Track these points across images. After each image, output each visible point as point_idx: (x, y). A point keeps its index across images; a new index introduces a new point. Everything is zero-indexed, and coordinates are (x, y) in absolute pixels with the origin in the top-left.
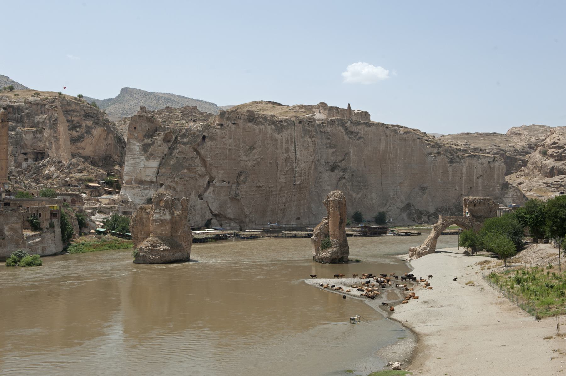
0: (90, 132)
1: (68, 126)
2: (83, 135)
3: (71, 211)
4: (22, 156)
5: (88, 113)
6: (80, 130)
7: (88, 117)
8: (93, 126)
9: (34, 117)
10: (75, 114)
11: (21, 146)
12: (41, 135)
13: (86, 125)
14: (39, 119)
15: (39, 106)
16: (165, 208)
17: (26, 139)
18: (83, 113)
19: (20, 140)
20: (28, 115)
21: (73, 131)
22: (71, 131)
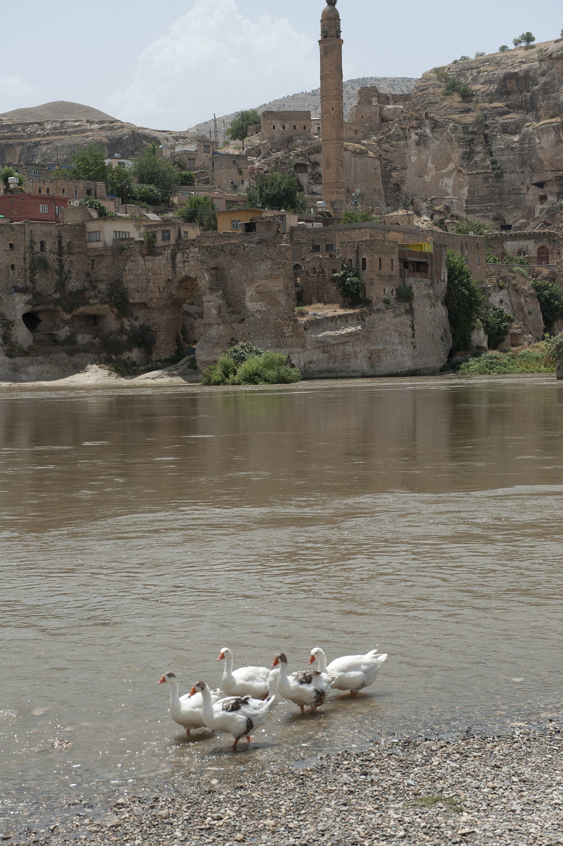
3: (522, 275)
11: (531, 166)
19: (529, 153)
20: (547, 89)
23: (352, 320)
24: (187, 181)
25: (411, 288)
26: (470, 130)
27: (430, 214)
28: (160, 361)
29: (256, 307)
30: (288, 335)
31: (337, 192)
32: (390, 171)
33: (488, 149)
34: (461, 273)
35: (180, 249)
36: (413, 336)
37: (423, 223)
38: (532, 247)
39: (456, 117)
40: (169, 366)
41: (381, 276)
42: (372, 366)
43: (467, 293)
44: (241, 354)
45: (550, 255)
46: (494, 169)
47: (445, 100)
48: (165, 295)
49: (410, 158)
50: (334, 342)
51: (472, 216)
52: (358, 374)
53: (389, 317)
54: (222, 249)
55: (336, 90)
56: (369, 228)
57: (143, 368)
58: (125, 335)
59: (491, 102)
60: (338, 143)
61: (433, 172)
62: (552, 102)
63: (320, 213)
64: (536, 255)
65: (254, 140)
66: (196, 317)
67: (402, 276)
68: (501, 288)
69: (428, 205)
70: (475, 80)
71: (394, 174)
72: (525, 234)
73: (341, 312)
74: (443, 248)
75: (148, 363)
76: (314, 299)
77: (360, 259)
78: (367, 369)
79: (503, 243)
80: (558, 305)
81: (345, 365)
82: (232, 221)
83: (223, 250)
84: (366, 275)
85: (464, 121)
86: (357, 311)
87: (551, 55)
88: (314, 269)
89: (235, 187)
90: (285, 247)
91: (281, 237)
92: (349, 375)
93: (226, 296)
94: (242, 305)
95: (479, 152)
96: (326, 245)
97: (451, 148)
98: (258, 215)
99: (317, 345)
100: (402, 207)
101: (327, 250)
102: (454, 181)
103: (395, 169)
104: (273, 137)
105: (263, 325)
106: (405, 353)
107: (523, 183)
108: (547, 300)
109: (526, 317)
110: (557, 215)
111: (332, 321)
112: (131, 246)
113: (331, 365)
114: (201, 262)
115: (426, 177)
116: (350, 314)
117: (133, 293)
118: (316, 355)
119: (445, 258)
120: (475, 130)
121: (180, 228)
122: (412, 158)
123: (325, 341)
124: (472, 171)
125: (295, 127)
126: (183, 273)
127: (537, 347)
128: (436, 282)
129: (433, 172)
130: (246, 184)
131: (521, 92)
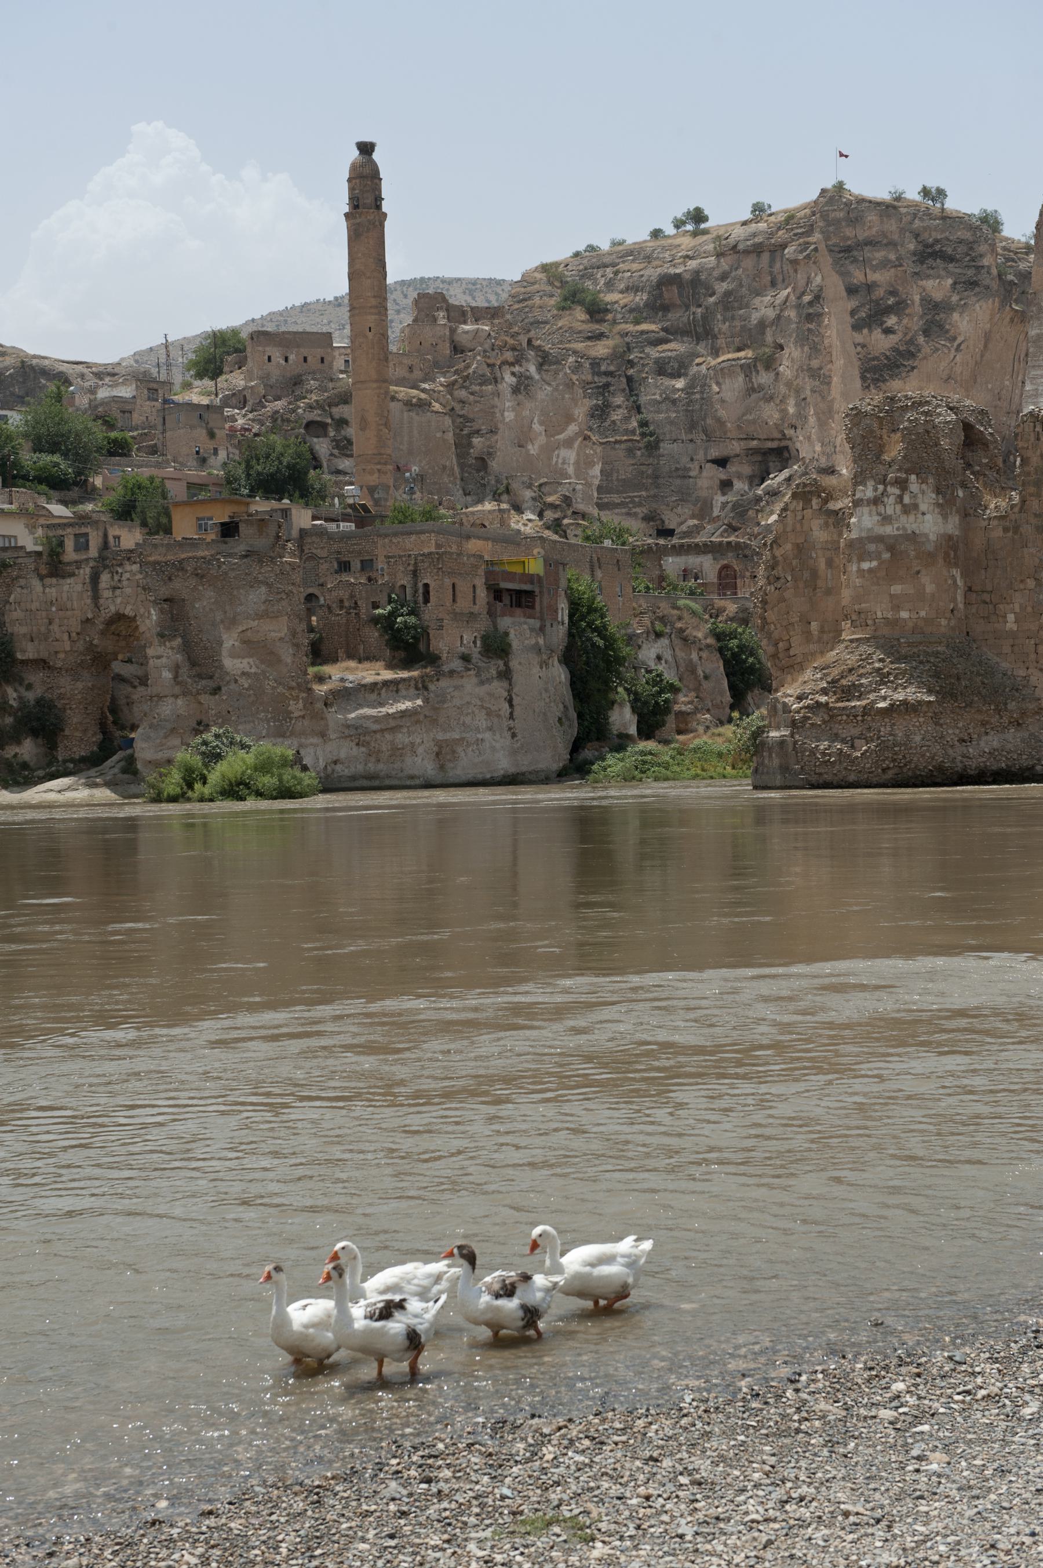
0: (941, 327)
1: (853, 313)
2: (911, 342)
3: (694, 613)
4: (711, 470)
5: (932, 246)
6: (898, 323)
7: (930, 261)
8: (955, 298)
9: (747, 306)
10: (880, 255)
11: (705, 431)
12: (772, 375)
13: (922, 300)
14: (763, 311)
15: (766, 257)
16: (908, 472)
17: (723, 401)
18: (912, 247)
19: (701, 409)
20: (730, 303)
21: (870, 331)
22: (865, 331)
23: (407, 689)
24: (118, 449)
25: (507, 634)
26: (603, 368)
27: (538, 509)
28: (72, 760)
29: (242, 666)
30: (296, 714)
31: (379, 470)
32: (470, 436)
33: (634, 402)
34: (591, 610)
35: (105, 567)
36: (511, 716)
37: (525, 525)
38: (709, 566)
39: (579, 346)
40: (89, 769)
41: (455, 614)
42: (442, 767)
43: (601, 643)
44: (214, 748)
45: (738, 581)
46: (643, 435)
47: (560, 317)
48: (80, 646)
49: (502, 415)
50: (376, 727)
51: (608, 512)
52: (417, 782)
53: (470, 683)
54: (180, 566)
55: (375, 297)
56: (434, 532)
57: (40, 773)
58: (10, 715)
59: (637, 322)
60: (379, 388)
61: (542, 440)
62: (737, 323)
63: (350, 506)
64: (715, 580)
65: (235, 380)
66: (136, 684)
67: (491, 613)
68: (659, 635)
69: (533, 494)
70: (610, 285)
71: (476, 441)
72: (697, 545)
73: (388, 675)
74: (561, 568)
75: (50, 764)
76: (341, 653)
77: (420, 585)
78: (433, 773)
79: (660, 559)
80: (753, 664)
81: (395, 766)
82: (198, 519)
83: (183, 569)
84: (430, 613)
85: (593, 353)
86: (415, 673)
87: (735, 246)
88: (341, 601)
89: (203, 461)
90: (290, 564)
91: (284, 547)
92: (403, 783)
93: (187, 648)
94: (216, 664)
95: (619, 407)
96: (362, 561)
97: (573, 399)
98: (243, 509)
99: (347, 732)
100: (490, 497)
101: (363, 569)
102: (578, 455)
103: (478, 432)
104: (268, 376)
105: (252, 698)
106: (498, 745)
107: (692, 460)
108: (735, 656)
109: (700, 685)
110: (750, 512)
111: (373, 691)
112: (20, 560)
113: (371, 767)
114: (144, 589)
115: (530, 447)
116: (403, 680)
117: (24, 643)
118: (346, 750)
119: (563, 584)
120: (612, 368)
121: (105, 529)
122: (506, 414)
123: (361, 726)
124: (607, 437)
125: (305, 359)
126: (113, 609)
127: (719, 735)
128: (548, 625)
129: (542, 440)
130: (222, 455)
131: (687, 307)
